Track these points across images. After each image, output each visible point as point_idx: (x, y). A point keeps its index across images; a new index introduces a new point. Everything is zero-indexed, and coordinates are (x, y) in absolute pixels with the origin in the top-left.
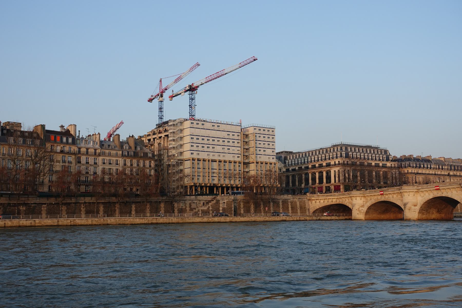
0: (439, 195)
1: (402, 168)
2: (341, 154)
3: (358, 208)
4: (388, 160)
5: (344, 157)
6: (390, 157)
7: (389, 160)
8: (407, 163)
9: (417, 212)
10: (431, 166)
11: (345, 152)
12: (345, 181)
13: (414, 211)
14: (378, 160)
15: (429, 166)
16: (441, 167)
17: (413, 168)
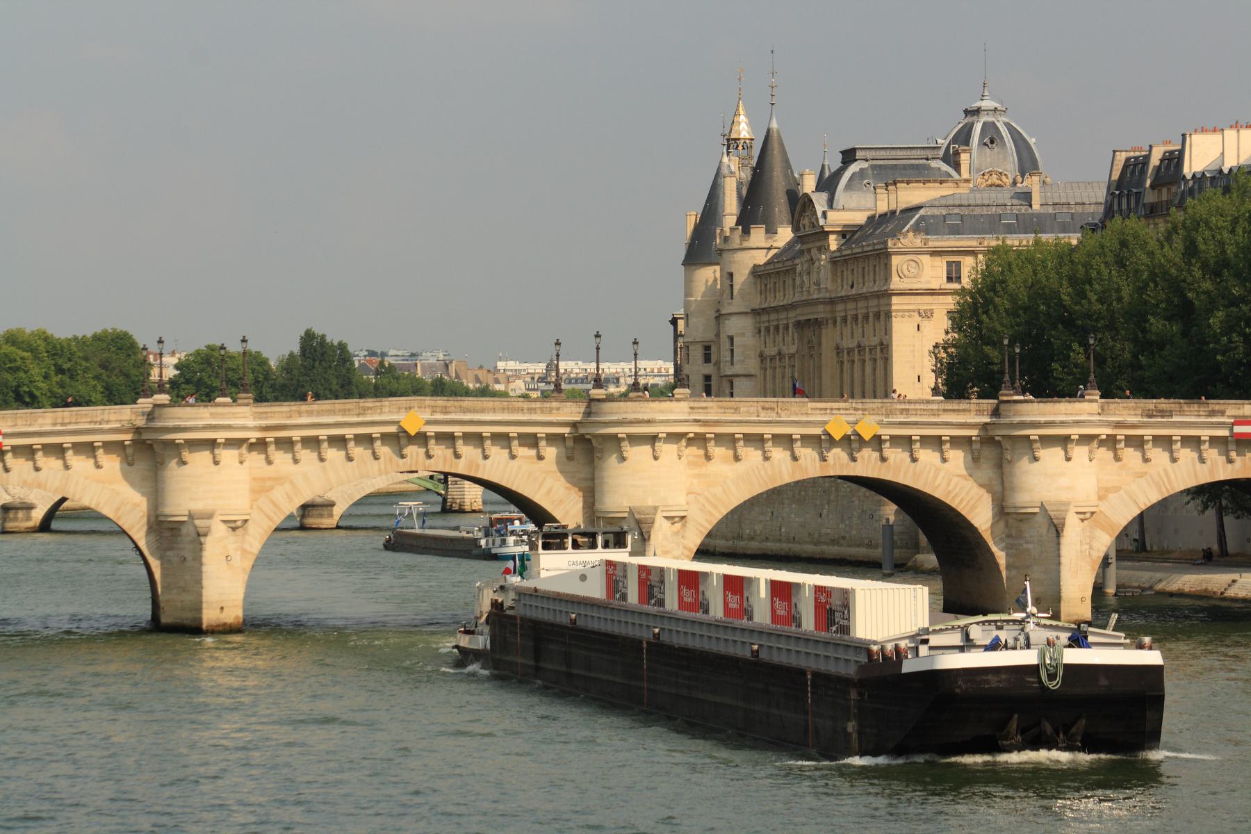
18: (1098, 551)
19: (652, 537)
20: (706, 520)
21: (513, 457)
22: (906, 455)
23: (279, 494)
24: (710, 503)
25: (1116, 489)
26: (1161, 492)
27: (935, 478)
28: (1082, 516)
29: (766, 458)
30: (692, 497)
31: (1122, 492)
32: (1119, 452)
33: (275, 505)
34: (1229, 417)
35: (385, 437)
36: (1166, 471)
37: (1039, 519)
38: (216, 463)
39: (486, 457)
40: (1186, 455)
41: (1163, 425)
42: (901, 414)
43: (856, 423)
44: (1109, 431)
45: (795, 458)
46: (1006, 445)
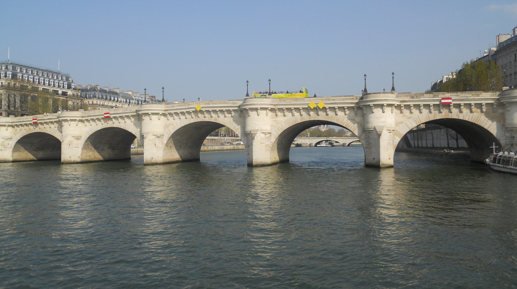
0: (109, 126)
1: (87, 98)
2: (6, 74)
3: (3, 142)
4: (69, 87)
5: (11, 78)
6: (72, 84)
7: (71, 88)
8: (93, 93)
9: (80, 147)
10: (118, 99)
11: (11, 73)
12: (9, 107)
13: (76, 147)
14: (57, 86)
15: (116, 99)
16: (128, 101)
17: (98, 99)
18: (396, 143)
19: (255, 139)
20: (277, 134)
21: (225, 117)
22: (334, 113)
23: (170, 128)
24: (278, 129)
25: (402, 123)
26: (416, 123)
27: (343, 120)
28: (389, 131)
29: (293, 115)
30: (272, 127)
31: (403, 123)
32: (402, 111)
33: (170, 131)
34: (440, 98)
35: (193, 112)
36: (418, 116)
37: (374, 132)
38: (151, 120)
39: (219, 117)
40: (425, 111)
41: (417, 101)
42: (333, 100)
43: (317, 104)
44: (399, 103)
45: (301, 115)
46: (364, 108)
